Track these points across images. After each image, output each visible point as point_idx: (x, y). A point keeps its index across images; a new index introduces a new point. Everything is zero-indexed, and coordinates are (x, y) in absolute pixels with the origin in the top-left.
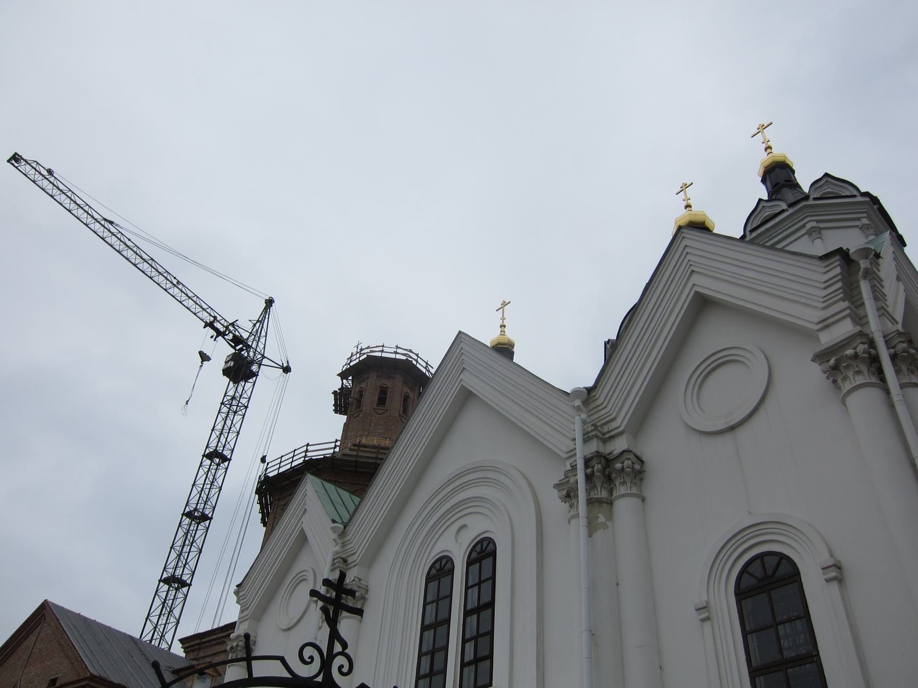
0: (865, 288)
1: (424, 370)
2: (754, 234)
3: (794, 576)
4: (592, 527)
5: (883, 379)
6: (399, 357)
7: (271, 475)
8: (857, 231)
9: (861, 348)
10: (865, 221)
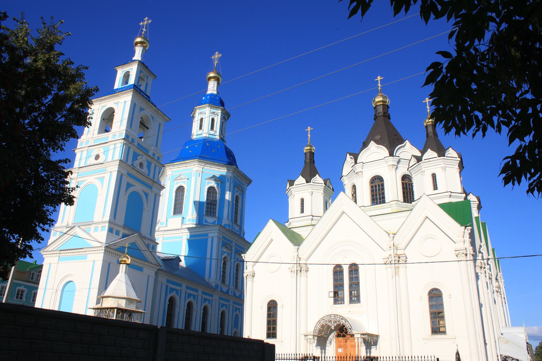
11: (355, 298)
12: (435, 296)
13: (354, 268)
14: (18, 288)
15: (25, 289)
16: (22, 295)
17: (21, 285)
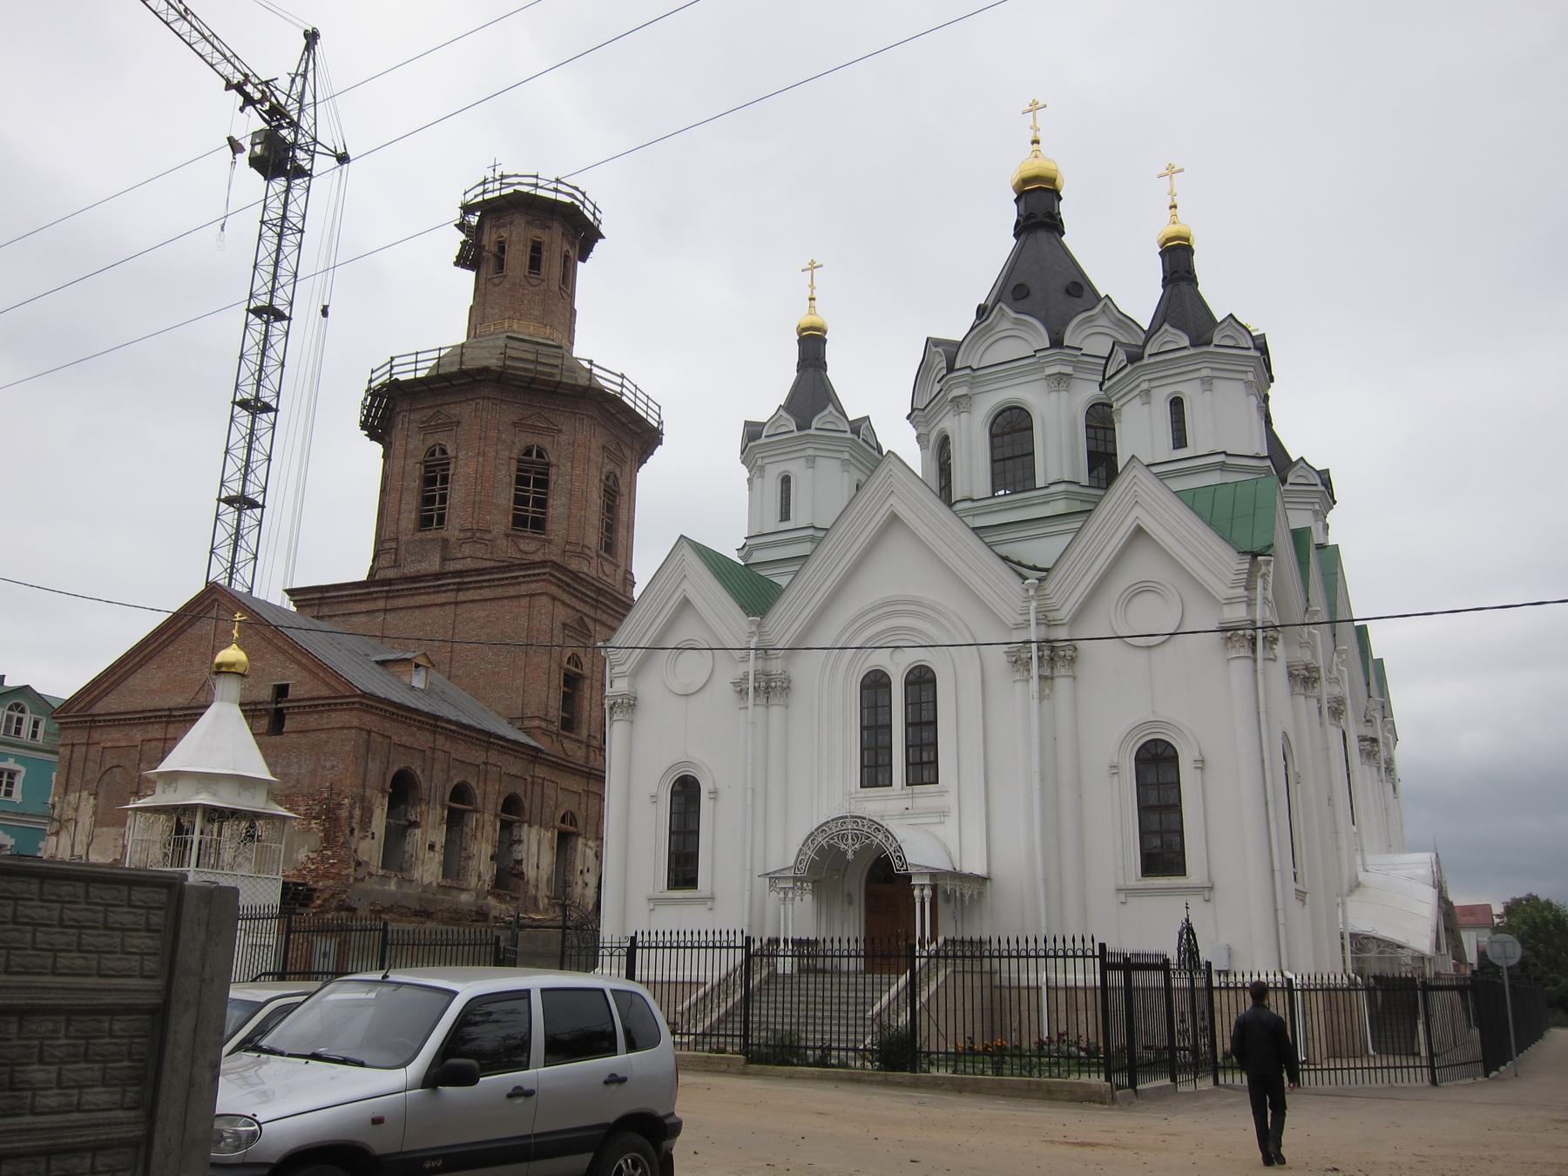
1: (591, 218)
2: (1152, 360)
3: (1174, 759)
4: (1042, 697)
5: (1254, 651)
6: (561, 198)
7: (402, 378)
8: (1241, 384)
9: (1249, 632)
10: (1251, 377)
11: (923, 769)
12: (1156, 763)
13: (922, 681)
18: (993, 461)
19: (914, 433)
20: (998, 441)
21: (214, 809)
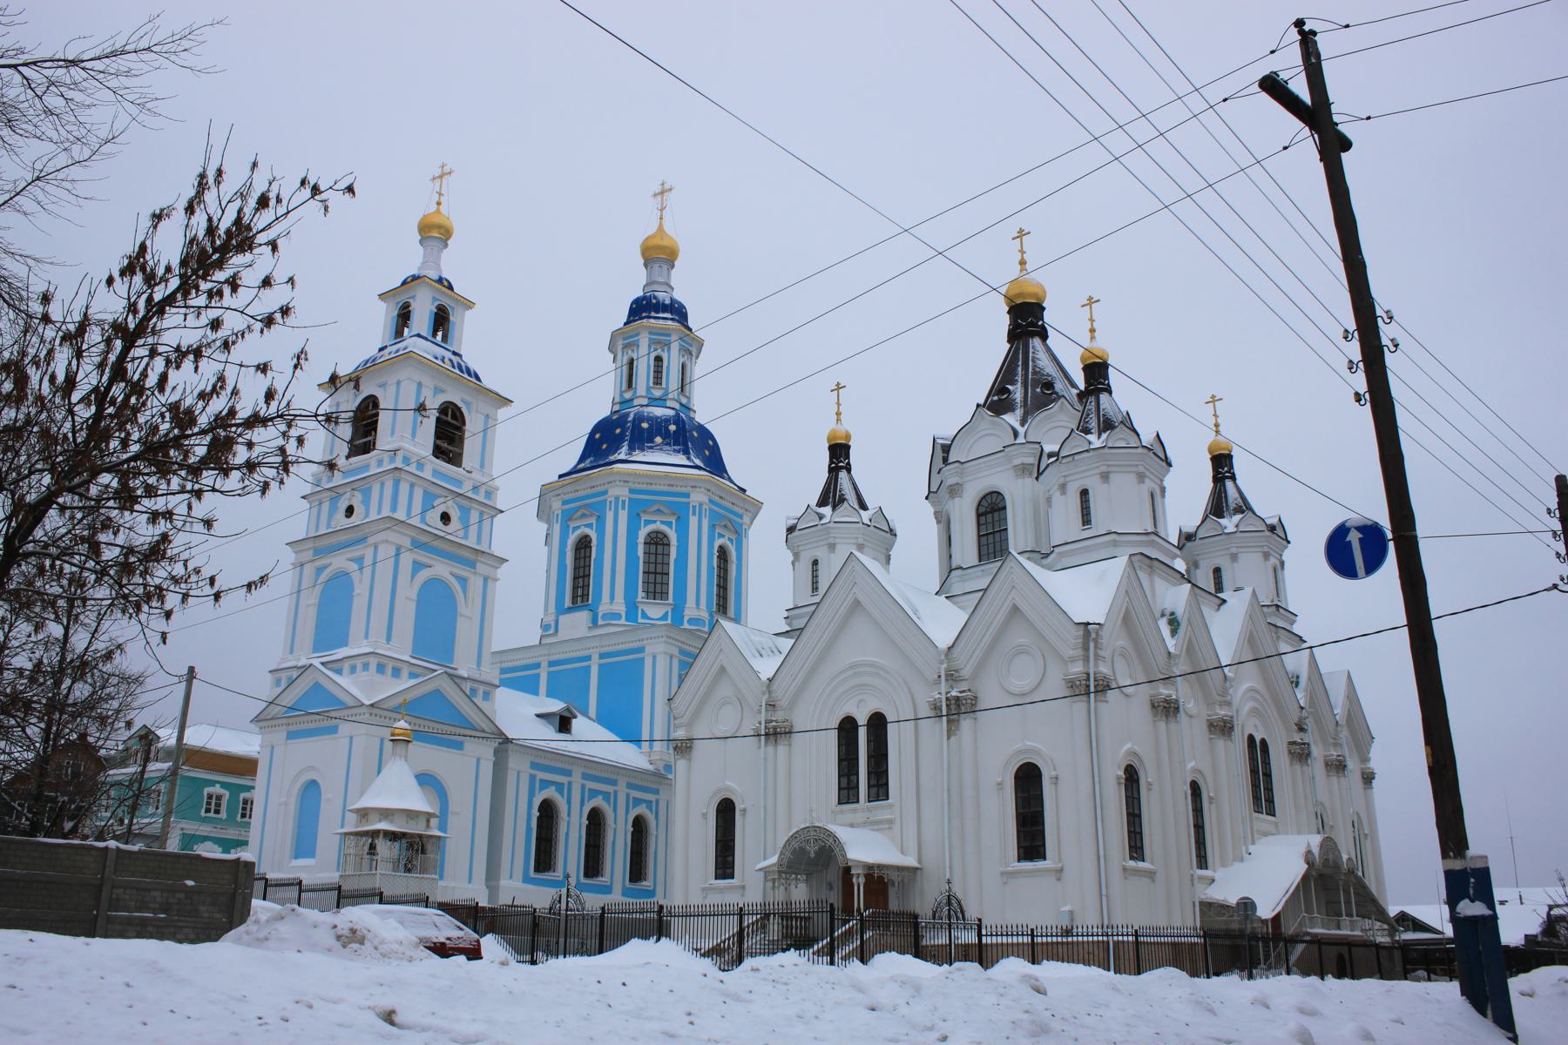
0: (1092, 645)
11: (880, 788)
12: (1028, 780)
13: (878, 723)
14: (207, 790)
15: (222, 791)
16: (218, 805)
17: (213, 783)
18: (979, 536)
19: (932, 510)
20: (983, 519)
21: (393, 833)
